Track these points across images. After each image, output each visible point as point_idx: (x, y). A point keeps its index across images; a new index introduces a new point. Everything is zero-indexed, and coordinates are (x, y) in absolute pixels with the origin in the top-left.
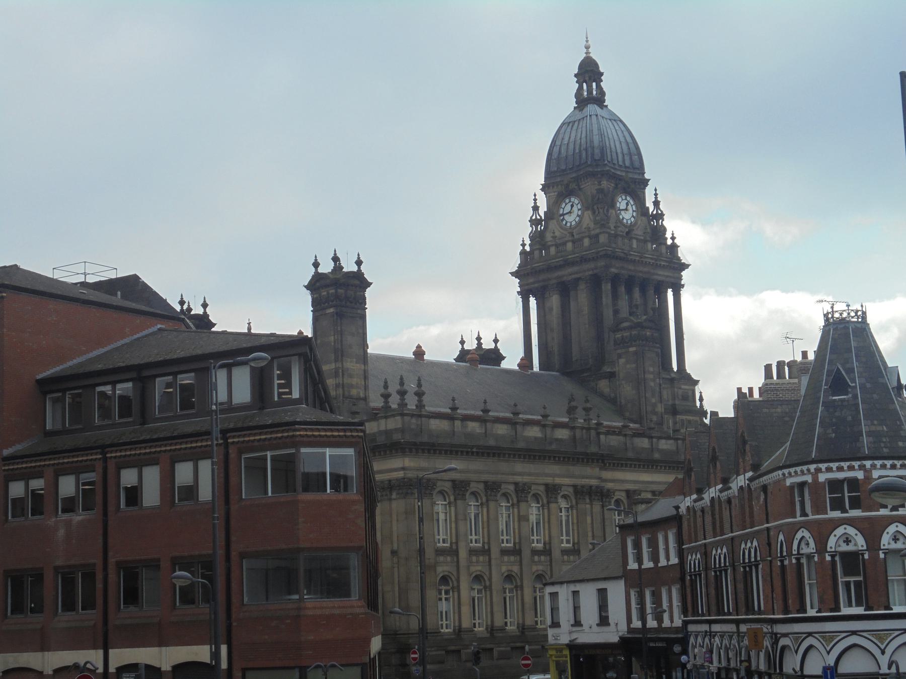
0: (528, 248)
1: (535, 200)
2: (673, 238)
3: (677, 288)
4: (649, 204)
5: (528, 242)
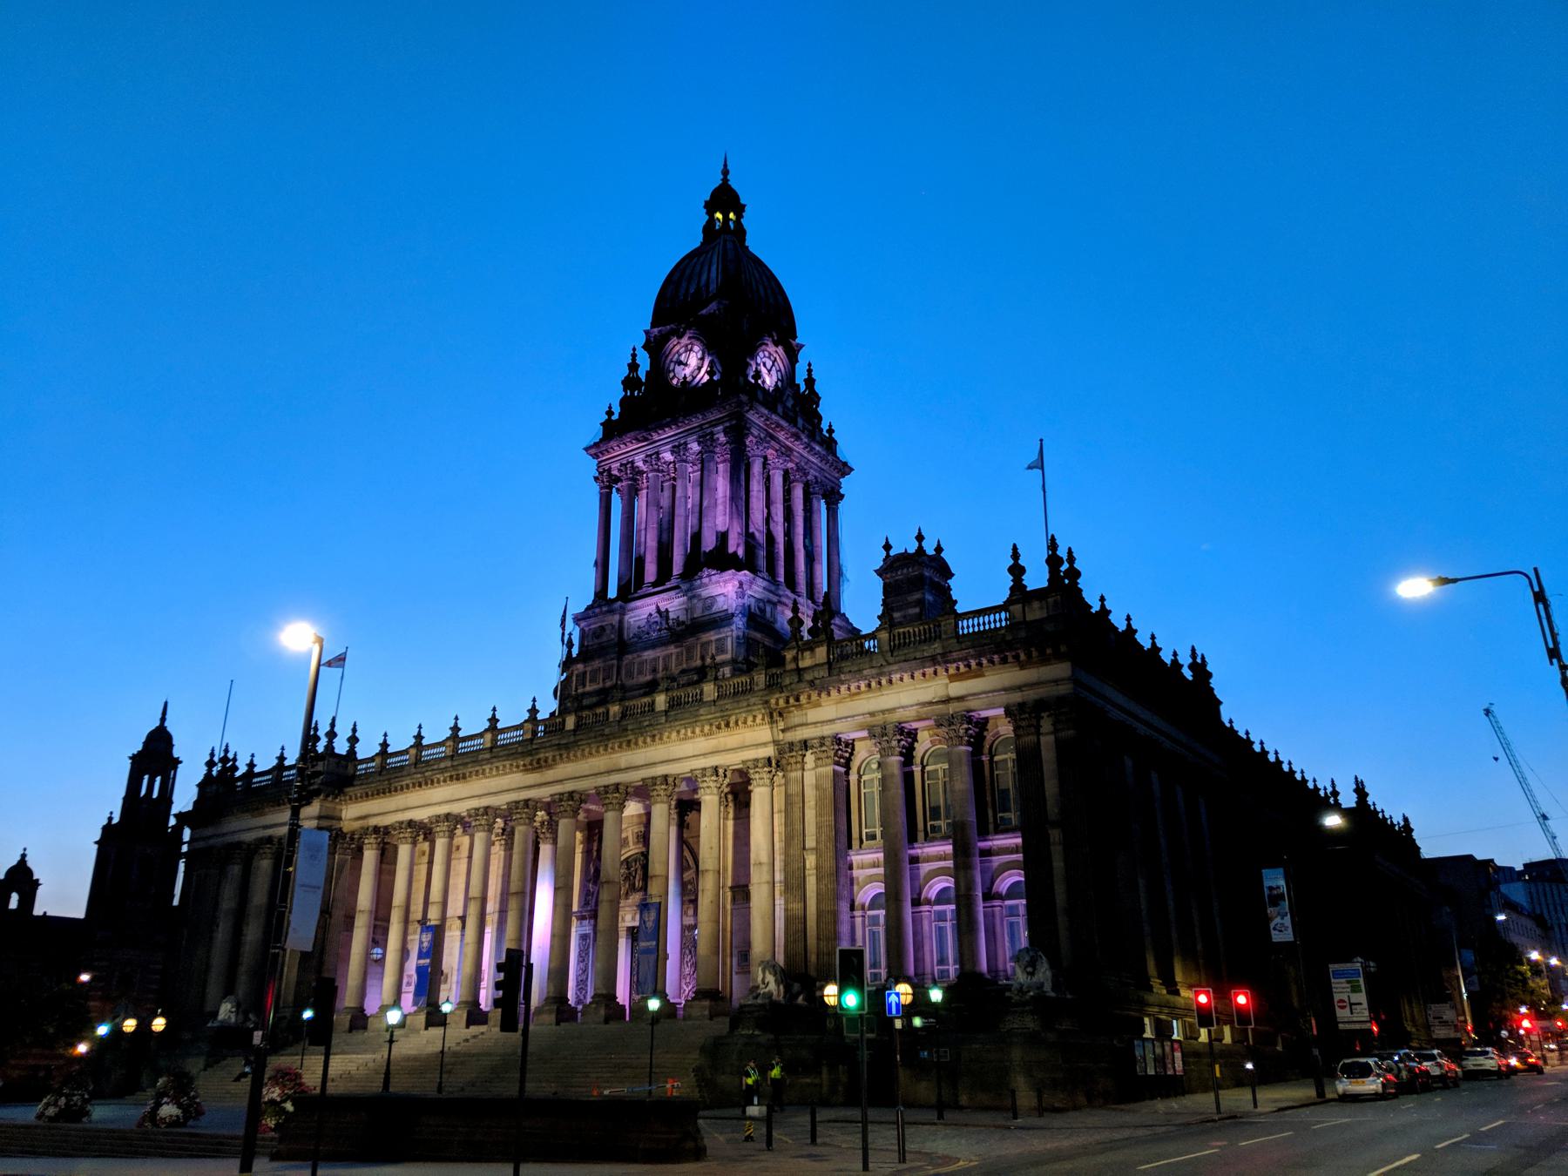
0: (615, 417)
1: (634, 356)
2: (831, 431)
3: (834, 497)
4: (800, 378)
5: (617, 410)
